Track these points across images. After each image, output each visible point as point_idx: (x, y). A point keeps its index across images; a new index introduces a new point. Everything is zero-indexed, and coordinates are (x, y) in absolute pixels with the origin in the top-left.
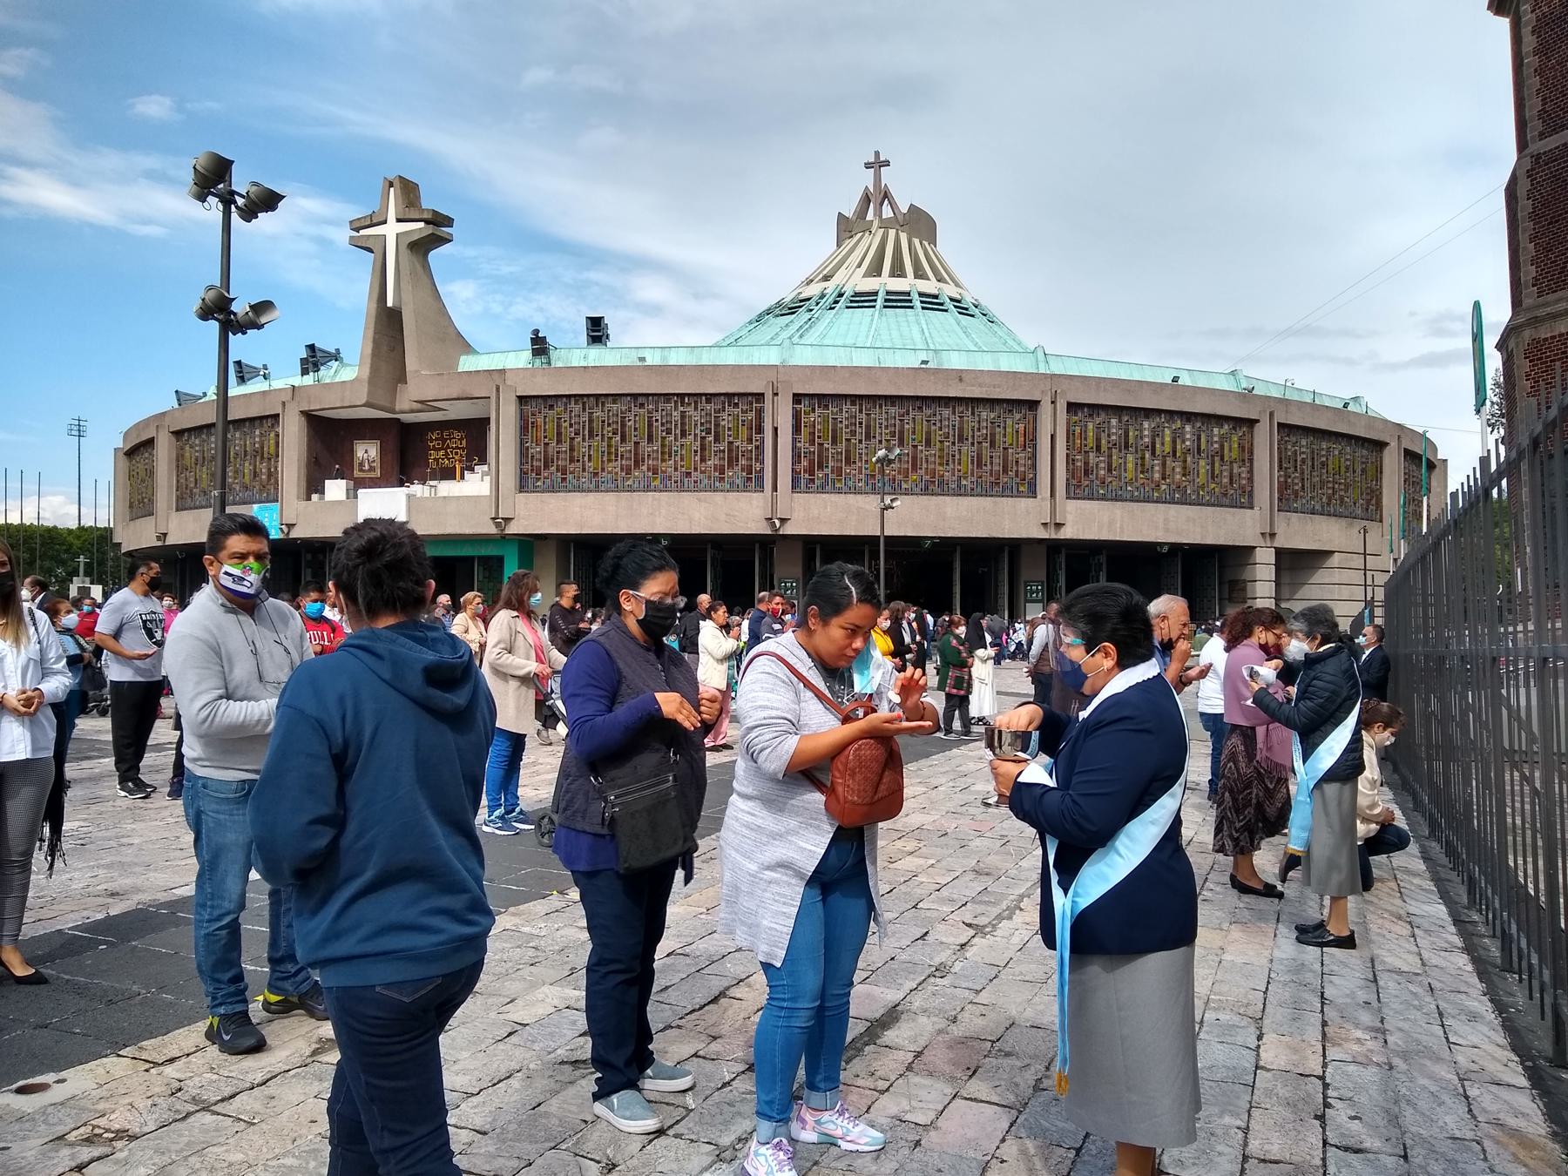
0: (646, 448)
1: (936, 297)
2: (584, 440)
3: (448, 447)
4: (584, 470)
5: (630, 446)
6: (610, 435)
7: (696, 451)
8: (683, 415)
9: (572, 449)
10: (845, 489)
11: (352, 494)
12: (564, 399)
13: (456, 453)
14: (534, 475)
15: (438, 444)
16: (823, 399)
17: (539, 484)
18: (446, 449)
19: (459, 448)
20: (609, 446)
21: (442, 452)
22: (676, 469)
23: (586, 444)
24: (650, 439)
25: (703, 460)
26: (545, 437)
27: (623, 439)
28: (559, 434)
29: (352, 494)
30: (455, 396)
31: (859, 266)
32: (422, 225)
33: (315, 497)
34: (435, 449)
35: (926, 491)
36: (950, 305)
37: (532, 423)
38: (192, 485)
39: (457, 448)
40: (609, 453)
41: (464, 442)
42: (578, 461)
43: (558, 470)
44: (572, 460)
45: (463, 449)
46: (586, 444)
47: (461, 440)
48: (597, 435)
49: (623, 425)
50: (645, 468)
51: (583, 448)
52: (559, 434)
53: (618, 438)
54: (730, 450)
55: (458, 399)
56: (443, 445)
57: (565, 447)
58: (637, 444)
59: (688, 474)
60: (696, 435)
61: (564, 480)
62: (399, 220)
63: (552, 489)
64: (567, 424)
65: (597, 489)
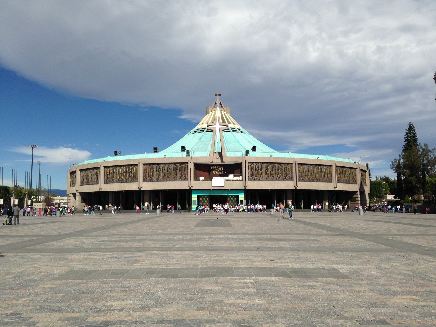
0: (272, 173)
1: (234, 128)
3: (218, 170)
5: (269, 172)
10: (260, 178)
16: (302, 164)
21: (217, 171)
24: (273, 171)
25: (282, 175)
27: (268, 171)
28: (255, 169)
34: (215, 170)
35: (317, 181)
36: (238, 131)
41: (222, 169)
44: (258, 175)
47: (222, 169)
49: (268, 168)
51: (260, 172)
52: (255, 169)
53: (267, 170)
54: (287, 173)
57: (257, 172)
59: (280, 178)
61: (256, 178)
62: (219, 125)
63: (254, 180)
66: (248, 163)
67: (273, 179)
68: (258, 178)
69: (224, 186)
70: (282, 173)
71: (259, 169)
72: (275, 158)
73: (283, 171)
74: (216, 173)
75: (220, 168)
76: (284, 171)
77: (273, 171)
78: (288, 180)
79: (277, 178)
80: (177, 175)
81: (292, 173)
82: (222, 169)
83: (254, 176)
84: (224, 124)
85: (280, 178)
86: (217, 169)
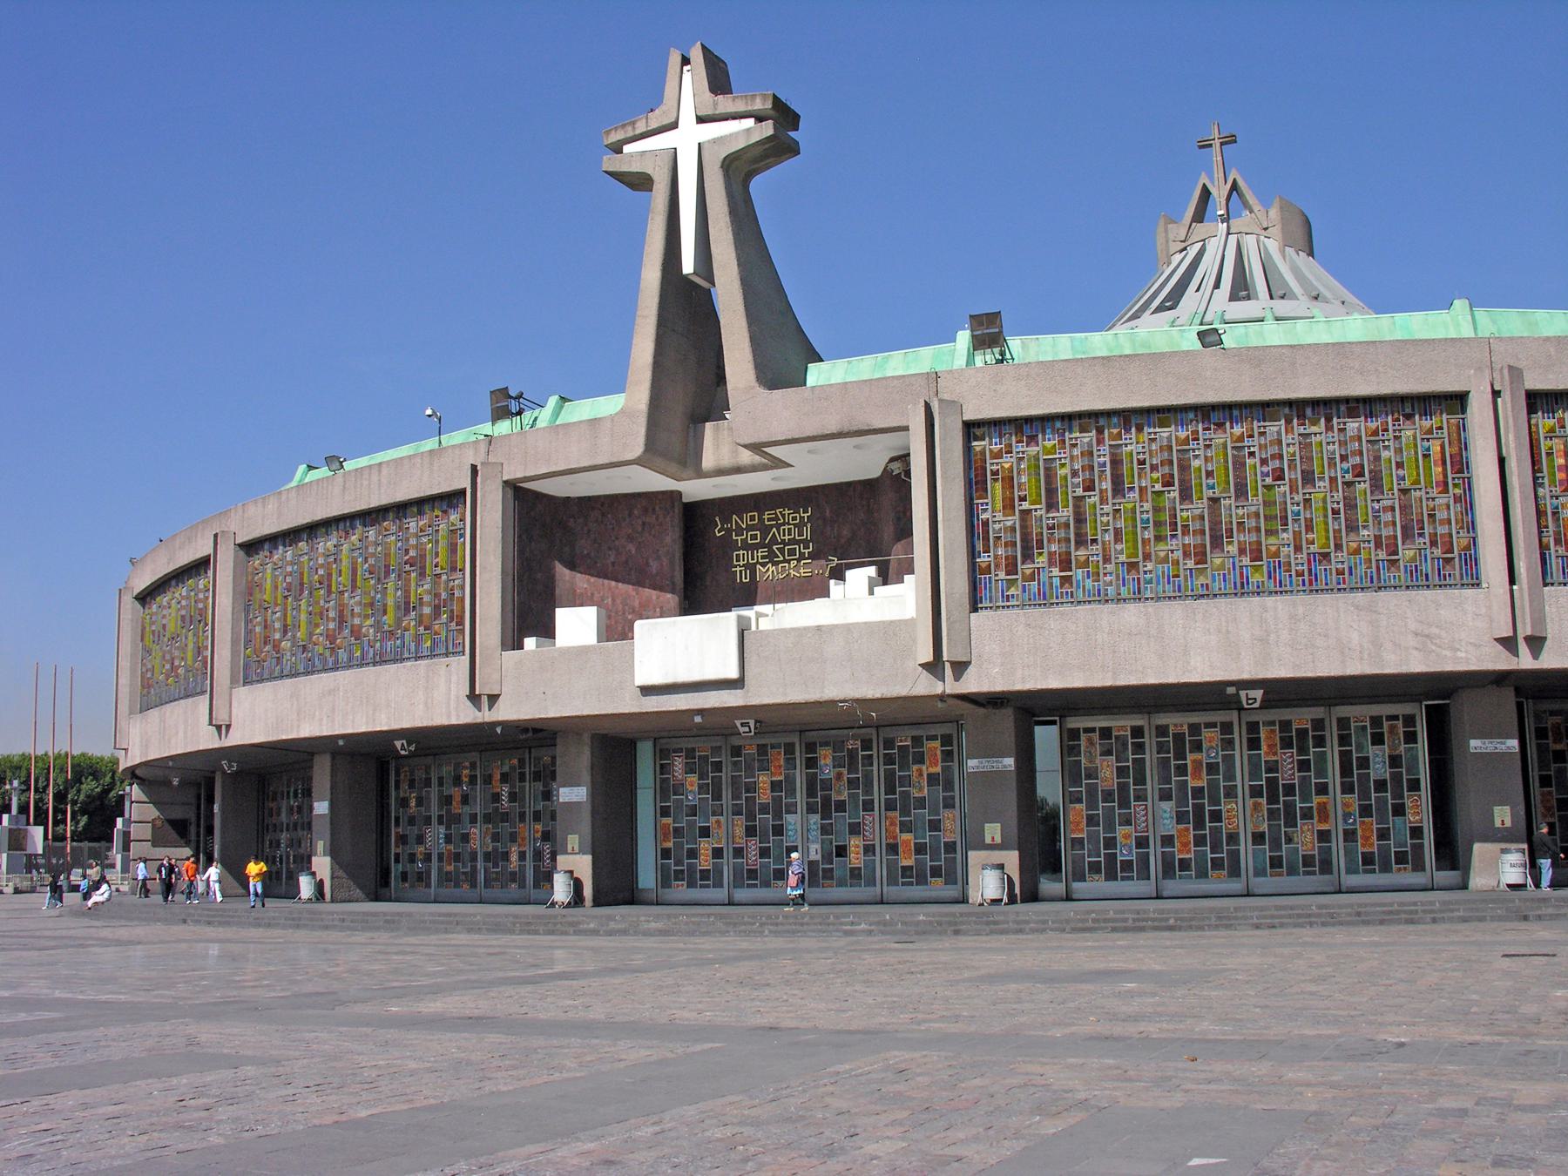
2: (1103, 501)
3: (774, 541)
4: (1107, 560)
5: (1200, 506)
6: (1158, 487)
7: (1336, 512)
8: (1305, 446)
9: (1080, 519)
11: (616, 629)
12: (1058, 424)
13: (792, 552)
14: (1002, 575)
15: (754, 537)
17: (1012, 591)
18: (769, 546)
19: (798, 542)
20: (1157, 510)
21: (760, 553)
22: (1298, 549)
23: (1108, 508)
24: (1241, 491)
25: (1352, 527)
26: (1023, 499)
27: (1186, 495)
28: (1051, 492)
29: (616, 629)
30: (833, 429)
31: (1217, 285)
32: (750, 122)
33: (530, 643)
34: (746, 546)
37: (995, 473)
38: (277, 636)
39: (793, 541)
40: (1158, 524)
41: (807, 533)
42: (1094, 541)
43: (1051, 563)
44: (1081, 541)
45: (806, 543)
46: (1108, 508)
47: (800, 526)
48: (1131, 489)
49: (1184, 467)
50: (1233, 549)
51: (1101, 510)
52: (1051, 492)
53: (1175, 494)
54: (1405, 509)
55: (840, 435)
56: (763, 538)
57: (1065, 513)
58: (1214, 501)
60: (1333, 480)
61: (1066, 580)
62: (701, 120)
63: (1044, 599)
64: (1065, 471)
65: (1138, 597)
66: (972, 429)
67: (1255, 578)
68: (1078, 574)
69: (732, 673)
70: (1350, 505)
71: (1089, 487)
72: (1256, 356)
73: (1363, 486)
74: (751, 568)
75: (791, 525)
76: (1377, 484)
77: (1241, 491)
78: (1418, 580)
79: (1299, 561)
80: (407, 611)
81: (1467, 502)
82: (800, 526)
83: (1041, 561)
84: (725, 104)
85: (1326, 556)
86: (765, 530)
